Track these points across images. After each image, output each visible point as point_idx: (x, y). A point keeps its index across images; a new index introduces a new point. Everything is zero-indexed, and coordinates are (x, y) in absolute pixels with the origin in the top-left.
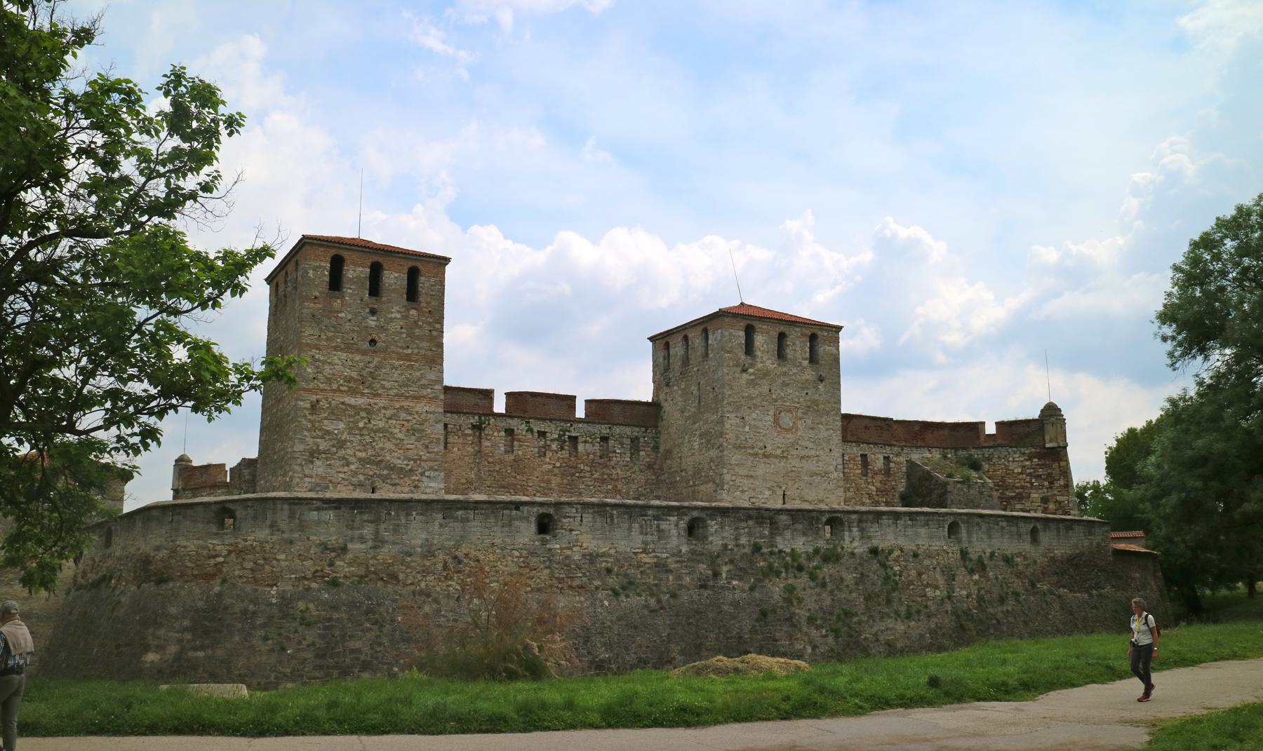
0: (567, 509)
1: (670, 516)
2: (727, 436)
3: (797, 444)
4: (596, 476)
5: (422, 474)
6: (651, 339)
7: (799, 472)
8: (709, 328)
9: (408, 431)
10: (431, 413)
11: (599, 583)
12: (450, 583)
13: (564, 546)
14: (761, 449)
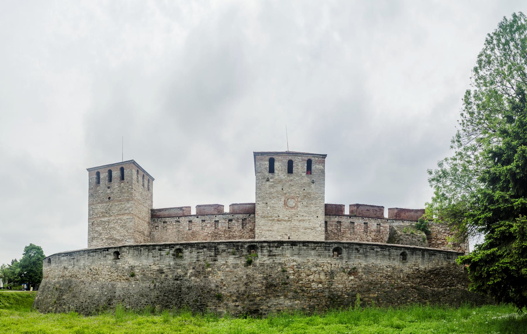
3: (298, 214)
9: (121, 226)
10: (128, 219)
14: (276, 217)
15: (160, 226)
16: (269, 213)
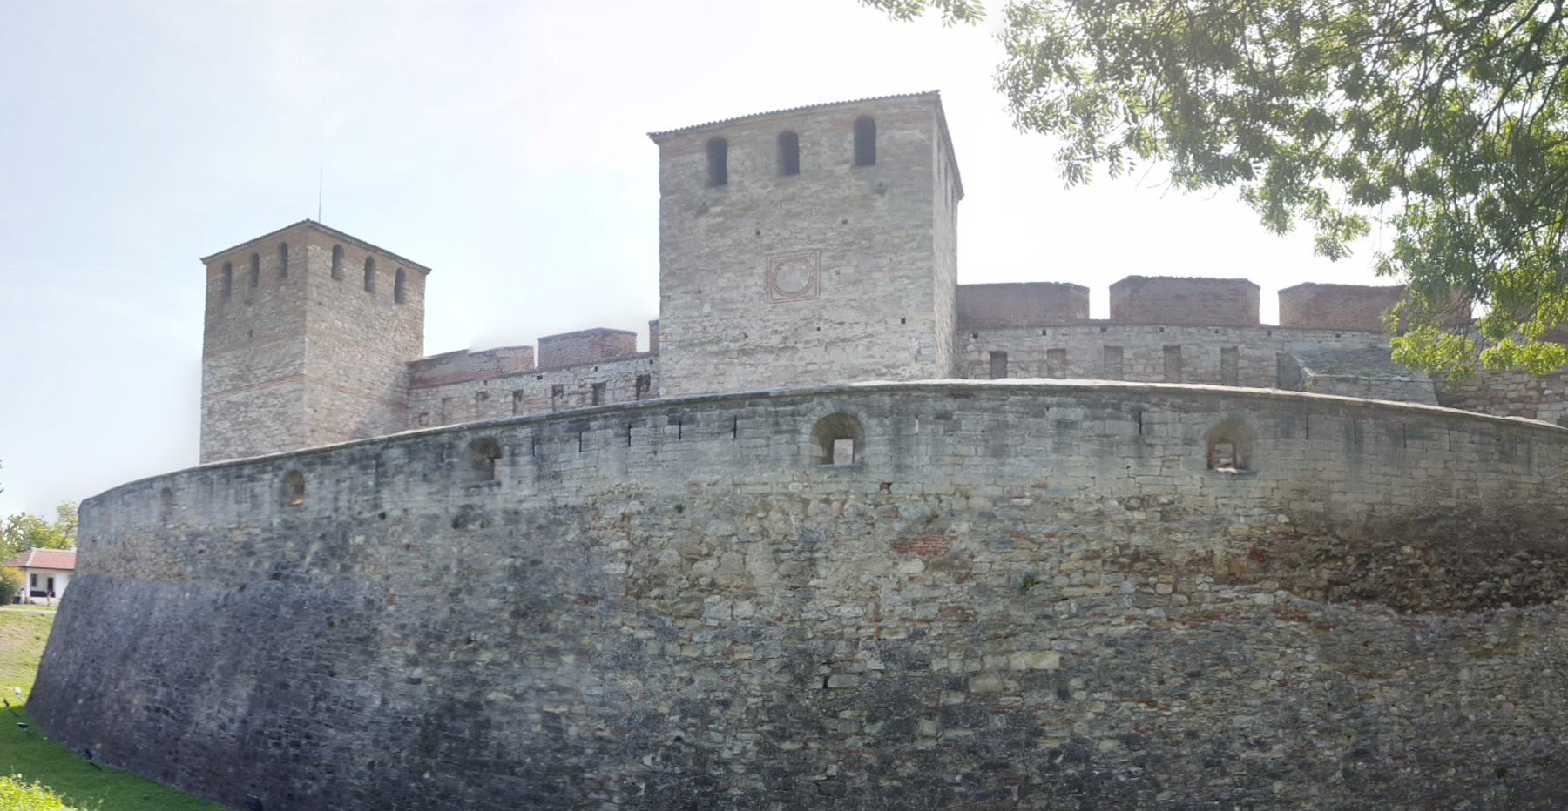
2: (667, 331)
14: (736, 340)
15: (432, 413)
16: (708, 329)
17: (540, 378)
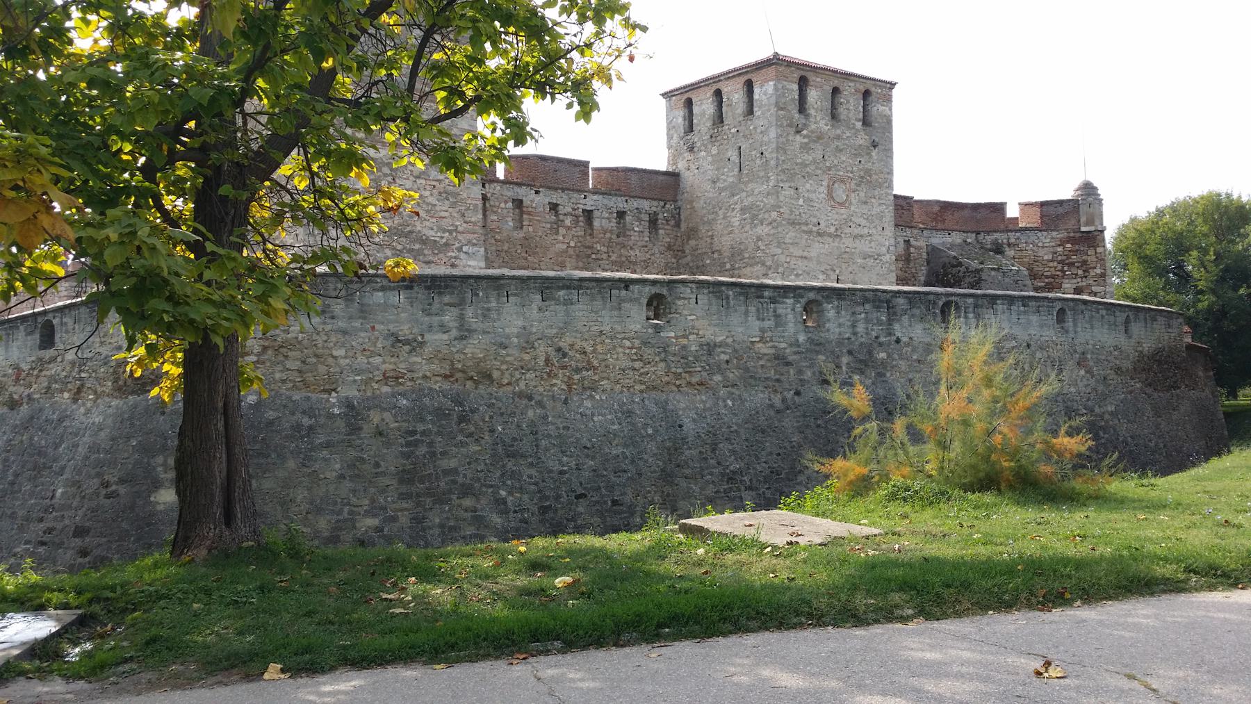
0: (681, 288)
1: (786, 298)
4: (613, 258)
5: (460, 249)
6: (664, 95)
7: (853, 253)
8: (754, 80)
9: (440, 193)
11: (720, 379)
12: (554, 381)
13: (679, 334)
14: (815, 226)
17: (537, 192)
